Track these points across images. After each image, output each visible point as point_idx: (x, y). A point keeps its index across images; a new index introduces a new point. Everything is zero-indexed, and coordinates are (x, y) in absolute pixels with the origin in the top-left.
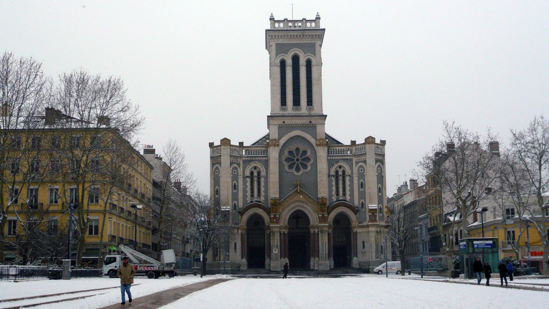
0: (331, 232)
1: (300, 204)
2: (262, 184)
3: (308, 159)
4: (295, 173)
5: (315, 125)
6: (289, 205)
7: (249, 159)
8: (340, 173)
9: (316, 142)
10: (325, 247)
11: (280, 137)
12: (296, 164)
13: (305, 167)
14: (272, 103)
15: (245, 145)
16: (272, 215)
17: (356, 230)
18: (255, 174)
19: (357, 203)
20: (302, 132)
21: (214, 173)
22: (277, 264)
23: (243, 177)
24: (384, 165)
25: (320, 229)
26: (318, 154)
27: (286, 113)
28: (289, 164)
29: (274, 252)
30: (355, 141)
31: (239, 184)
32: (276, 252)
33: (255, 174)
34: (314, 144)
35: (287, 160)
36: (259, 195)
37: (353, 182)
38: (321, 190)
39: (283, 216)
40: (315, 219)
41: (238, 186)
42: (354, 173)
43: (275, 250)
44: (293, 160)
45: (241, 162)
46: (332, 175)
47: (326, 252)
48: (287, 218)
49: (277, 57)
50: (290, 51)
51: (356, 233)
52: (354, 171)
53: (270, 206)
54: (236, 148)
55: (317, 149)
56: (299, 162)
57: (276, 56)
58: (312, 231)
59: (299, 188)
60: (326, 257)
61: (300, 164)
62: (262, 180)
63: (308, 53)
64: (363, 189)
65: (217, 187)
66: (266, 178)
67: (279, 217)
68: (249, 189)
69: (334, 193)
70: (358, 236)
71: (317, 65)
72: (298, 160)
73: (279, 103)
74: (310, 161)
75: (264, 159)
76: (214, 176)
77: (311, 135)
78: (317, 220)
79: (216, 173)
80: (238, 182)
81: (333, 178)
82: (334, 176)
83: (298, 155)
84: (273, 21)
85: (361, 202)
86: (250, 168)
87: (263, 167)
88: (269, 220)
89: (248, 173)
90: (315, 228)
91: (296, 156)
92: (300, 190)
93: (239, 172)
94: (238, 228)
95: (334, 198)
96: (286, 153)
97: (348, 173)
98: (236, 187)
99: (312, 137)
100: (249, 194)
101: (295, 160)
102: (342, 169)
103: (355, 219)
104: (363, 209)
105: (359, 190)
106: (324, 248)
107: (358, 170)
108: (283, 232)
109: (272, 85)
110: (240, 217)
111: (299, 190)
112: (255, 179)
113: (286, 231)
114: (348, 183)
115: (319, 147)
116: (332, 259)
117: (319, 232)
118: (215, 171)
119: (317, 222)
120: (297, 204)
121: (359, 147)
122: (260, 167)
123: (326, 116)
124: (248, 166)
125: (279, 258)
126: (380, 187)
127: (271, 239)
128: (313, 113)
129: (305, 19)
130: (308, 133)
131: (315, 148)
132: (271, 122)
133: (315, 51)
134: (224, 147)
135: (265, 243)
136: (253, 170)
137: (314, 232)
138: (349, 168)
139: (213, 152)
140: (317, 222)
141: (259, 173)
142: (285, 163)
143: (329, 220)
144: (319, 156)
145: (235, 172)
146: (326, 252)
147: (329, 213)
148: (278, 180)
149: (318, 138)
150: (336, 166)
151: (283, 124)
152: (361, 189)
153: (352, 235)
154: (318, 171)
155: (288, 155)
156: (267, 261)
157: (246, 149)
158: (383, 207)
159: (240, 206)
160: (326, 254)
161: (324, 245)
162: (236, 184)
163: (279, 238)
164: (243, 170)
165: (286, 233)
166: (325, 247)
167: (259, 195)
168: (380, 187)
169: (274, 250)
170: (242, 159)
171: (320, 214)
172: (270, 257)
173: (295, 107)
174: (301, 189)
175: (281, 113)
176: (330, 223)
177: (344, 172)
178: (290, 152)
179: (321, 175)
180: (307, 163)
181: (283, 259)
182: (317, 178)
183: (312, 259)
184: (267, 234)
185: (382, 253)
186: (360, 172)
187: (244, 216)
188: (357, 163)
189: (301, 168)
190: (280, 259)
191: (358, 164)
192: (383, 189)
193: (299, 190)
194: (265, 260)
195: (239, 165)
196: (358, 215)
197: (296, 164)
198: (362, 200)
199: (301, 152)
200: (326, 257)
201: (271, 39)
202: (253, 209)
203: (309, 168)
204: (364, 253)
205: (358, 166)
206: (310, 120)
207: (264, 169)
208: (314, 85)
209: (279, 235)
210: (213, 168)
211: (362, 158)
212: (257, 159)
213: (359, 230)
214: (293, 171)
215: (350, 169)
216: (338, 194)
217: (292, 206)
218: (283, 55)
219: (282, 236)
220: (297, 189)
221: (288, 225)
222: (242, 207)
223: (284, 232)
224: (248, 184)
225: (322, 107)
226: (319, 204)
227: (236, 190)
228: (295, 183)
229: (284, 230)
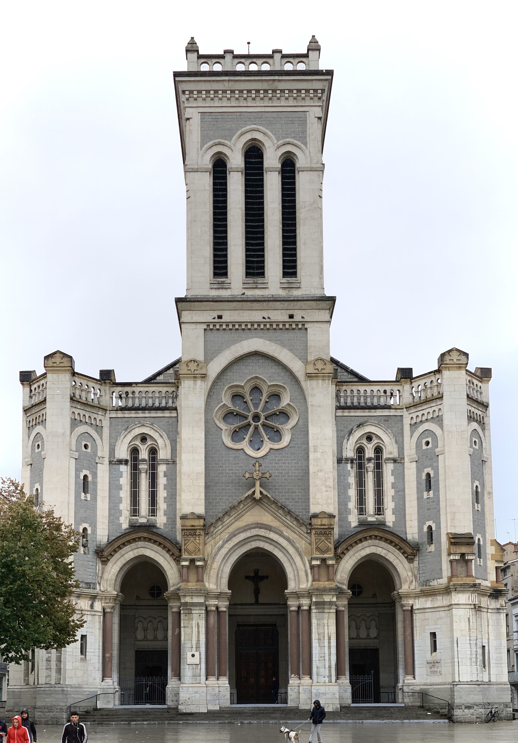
0: (343, 609)
1: (262, 532)
2: (162, 481)
3: (284, 415)
4: (250, 452)
5: (303, 325)
6: (233, 535)
9: (306, 369)
11: (210, 356)
12: (251, 429)
13: (277, 434)
14: (190, 266)
15: (119, 379)
16: (185, 560)
17: (411, 602)
19: (416, 530)
20: (268, 342)
21: (33, 450)
22: (196, 692)
23: (110, 462)
24: (487, 434)
25: (314, 600)
26: (310, 400)
27: (224, 293)
28: (232, 427)
29: (190, 660)
30: (410, 370)
31: (99, 479)
32: (196, 660)
33: (144, 454)
34: (300, 375)
35: (229, 415)
36: (153, 512)
37: (404, 478)
38: (319, 496)
39: (216, 565)
40: (302, 574)
41: (95, 484)
42: (406, 453)
43: (193, 656)
44: (246, 418)
45: (106, 423)
46: (347, 459)
47: (330, 659)
48: (227, 569)
49: (204, 149)
50: (239, 132)
51: (412, 610)
52: (406, 447)
53: (179, 538)
54: (91, 384)
55: (308, 385)
56: (259, 423)
57: (202, 147)
58: (293, 604)
59: (258, 488)
60: (330, 676)
61: (261, 428)
62: (162, 469)
63: (287, 138)
64: (431, 492)
65: (37, 486)
66: (172, 462)
67: (203, 567)
68: (125, 494)
69: (352, 505)
70: (417, 617)
71: (312, 170)
72: (256, 417)
73: (208, 268)
74: (290, 421)
75: (167, 414)
76: (33, 460)
77: (291, 350)
78: (307, 575)
79: (37, 451)
80: (95, 475)
82: (352, 461)
83: (256, 406)
84: (195, 55)
85: (425, 529)
86: (130, 437)
87: (165, 436)
88: (177, 575)
90: (303, 596)
91: (252, 408)
92: (261, 493)
93: (99, 448)
94: (94, 598)
95: (353, 520)
96: (226, 400)
98: (90, 486)
99: (296, 356)
100: (125, 506)
101: (250, 419)
102: (375, 441)
103: (410, 574)
104: (433, 546)
105: (420, 498)
106: (327, 651)
107: (418, 445)
108: (214, 608)
109: (191, 223)
110: (100, 566)
111: (258, 496)
112: (143, 467)
113: (224, 605)
114: (388, 479)
115: (314, 383)
116: (345, 680)
117: (313, 607)
118: (33, 446)
119: (307, 581)
120: (254, 532)
121: (422, 382)
122: (156, 435)
123: (333, 300)
124: (124, 433)
125: (203, 678)
126: (477, 487)
127: (182, 625)
128: (296, 293)
129: (280, 51)
130: (283, 345)
131: (303, 384)
132: (187, 316)
133: (304, 131)
135: (166, 638)
136: (138, 442)
137: (299, 607)
138: (393, 441)
139: (31, 397)
140: (307, 581)
141: (153, 451)
142: (222, 425)
143: (338, 577)
144: (312, 406)
146: (330, 659)
147: (338, 558)
148: (201, 468)
149: (311, 358)
150: (358, 434)
151: (217, 320)
152: (425, 493)
153: (400, 617)
154: (311, 444)
155: (230, 405)
156: (172, 683)
157: (119, 389)
158: (485, 540)
159: (99, 538)
160: (330, 667)
161: (326, 644)
162: (90, 479)
163: (202, 623)
164: (110, 445)
165: (224, 609)
167: (153, 512)
168: (477, 487)
170: (108, 415)
171: (316, 559)
172: (178, 675)
173: (250, 280)
174: (265, 492)
175: (214, 293)
176: (343, 584)
178: (237, 397)
179: (318, 455)
180: (280, 426)
181: (212, 680)
182: (308, 463)
183: (293, 681)
184: (173, 612)
185: (484, 667)
186: (424, 447)
187: (110, 564)
188: (414, 426)
189: (266, 438)
190: (207, 679)
191: (417, 428)
192: (486, 495)
193: (258, 496)
194: (165, 684)
195: (99, 429)
196: (416, 563)
197: (251, 429)
198: (430, 523)
199: (264, 398)
200: (330, 676)
201: (187, 99)
202: (133, 545)
203: (286, 439)
204: (433, 664)
205: (417, 434)
206: (291, 312)
207: (168, 442)
208: (301, 222)
209: (204, 616)
210: (29, 437)
211: (428, 410)
213: (418, 604)
214: (244, 445)
215: (396, 442)
216: (361, 511)
217: (242, 536)
218: (220, 144)
219: (213, 619)
220: (254, 493)
221: (229, 589)
222: (105, 540)
223: (217, 608)
224: (125, 481)
225: (321, 278)
226: (313, 532)
227: (88, 496)
228: (247, 475)
229: (216, 602)
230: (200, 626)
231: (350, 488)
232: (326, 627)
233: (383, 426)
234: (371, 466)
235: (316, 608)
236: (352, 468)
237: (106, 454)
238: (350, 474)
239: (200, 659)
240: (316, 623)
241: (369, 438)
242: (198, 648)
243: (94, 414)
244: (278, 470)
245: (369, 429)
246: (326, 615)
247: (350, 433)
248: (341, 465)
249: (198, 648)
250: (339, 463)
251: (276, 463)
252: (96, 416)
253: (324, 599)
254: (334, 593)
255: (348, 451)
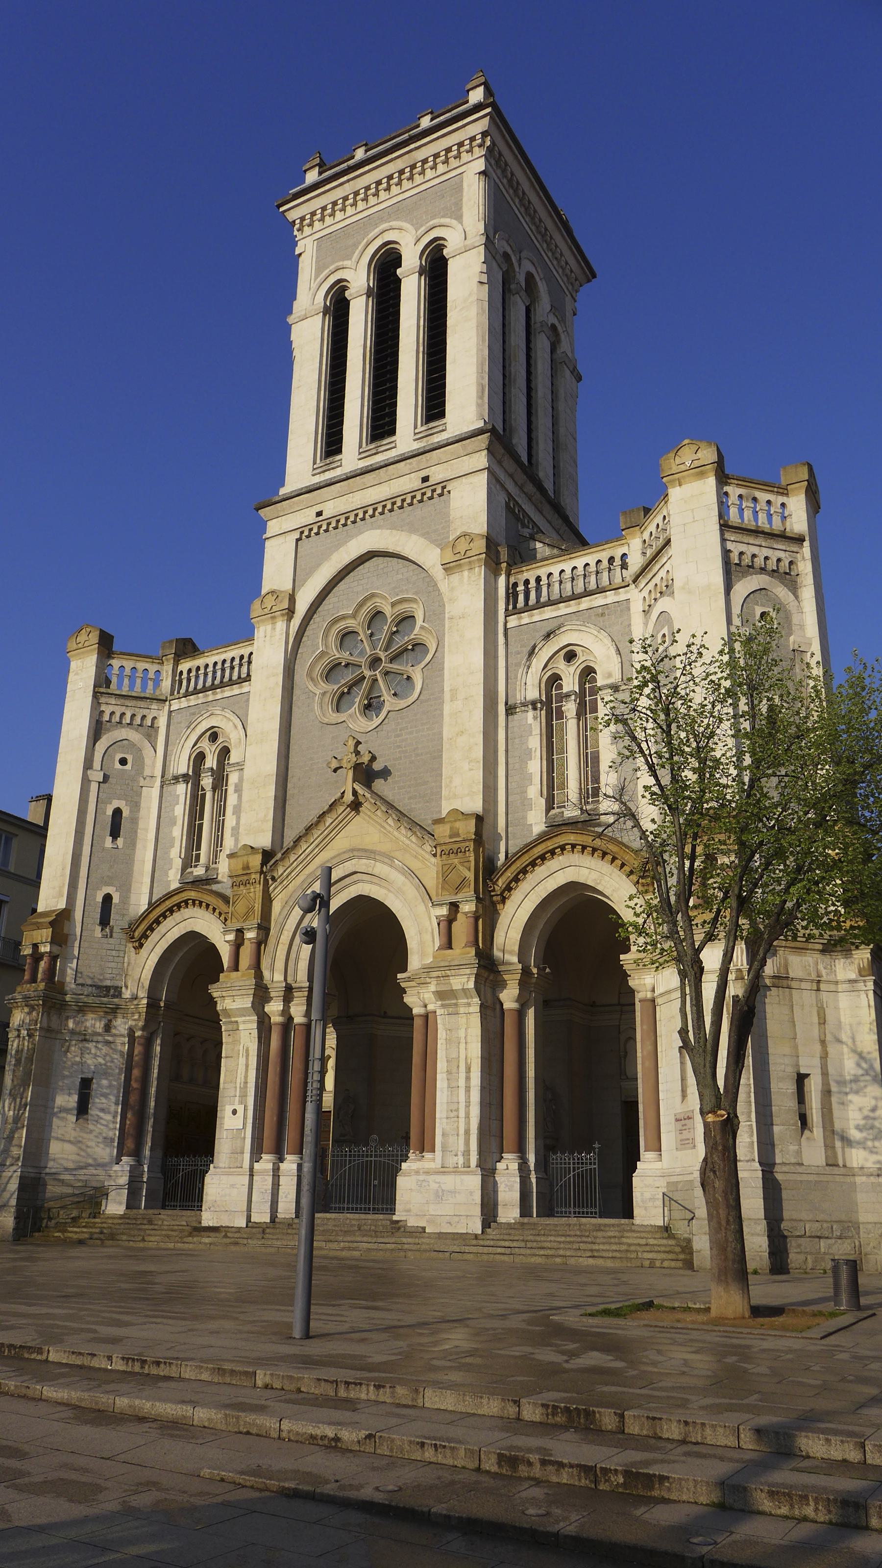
7: (192, 703)
8: (570, 683)
10: (468, 1089)
18: (211, 762)
46: (524, 704)
69: (534, 791)
81: (531, 714)
82: (534, 704)
89: (182, 765)
97: (610, 675)
134: (79, 662)
145: (123, 762)
166: (468, 1089)
169: (228, 1109)
170: (166, 708)
177: (588, 673)
212: (219, 696)
224: (180, 811)
230: (251, 1053)
231: (531, 759)
232: (462, 1046)
233: (578, 623)
234: (570, 708)
235: (443, 1006)
236: (535, 718)
237: (158, 773)
238: (531, 732)
239: (245, 1118)
240: (444, 1037)
241: (570, 656)
242: (244, 1096)
243: (141, 710)
244: (399, 747)
245: (563, 640)
246: (462, 1020)
247: (532, 653)
248: (516, 717)
249: (244, 1096)
250: (512, 714)
251: (398, 736)
252: (145, 712)
253: (451, 984)
254: (468, 971)
255: (529, 687)
